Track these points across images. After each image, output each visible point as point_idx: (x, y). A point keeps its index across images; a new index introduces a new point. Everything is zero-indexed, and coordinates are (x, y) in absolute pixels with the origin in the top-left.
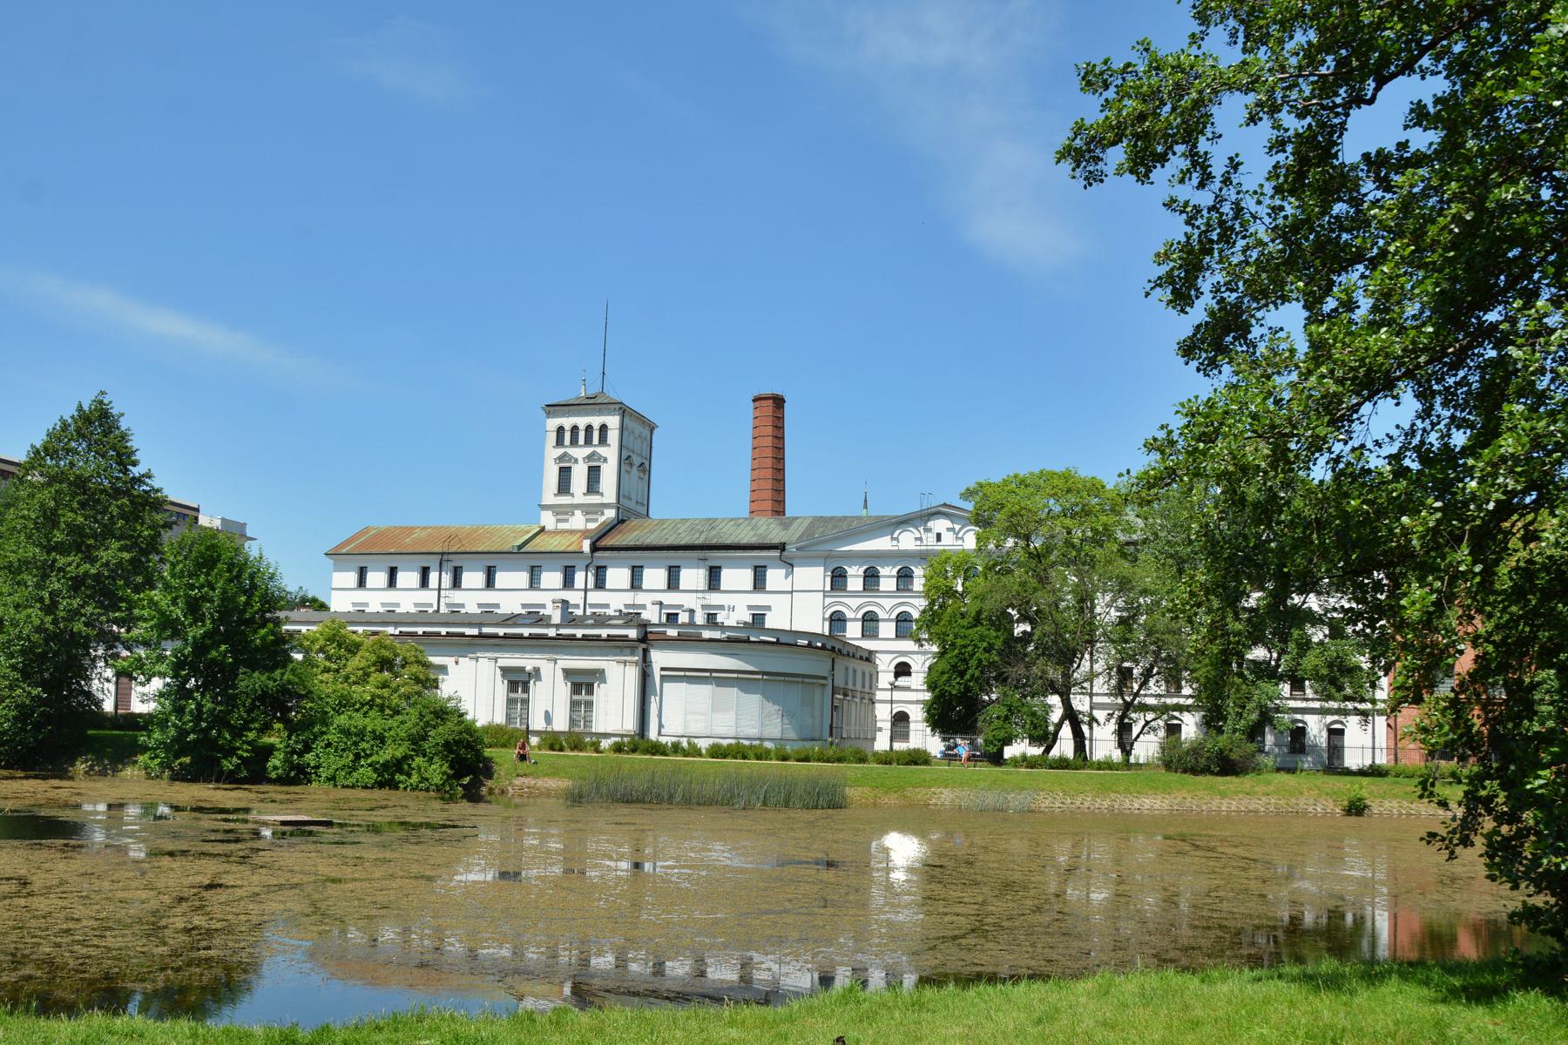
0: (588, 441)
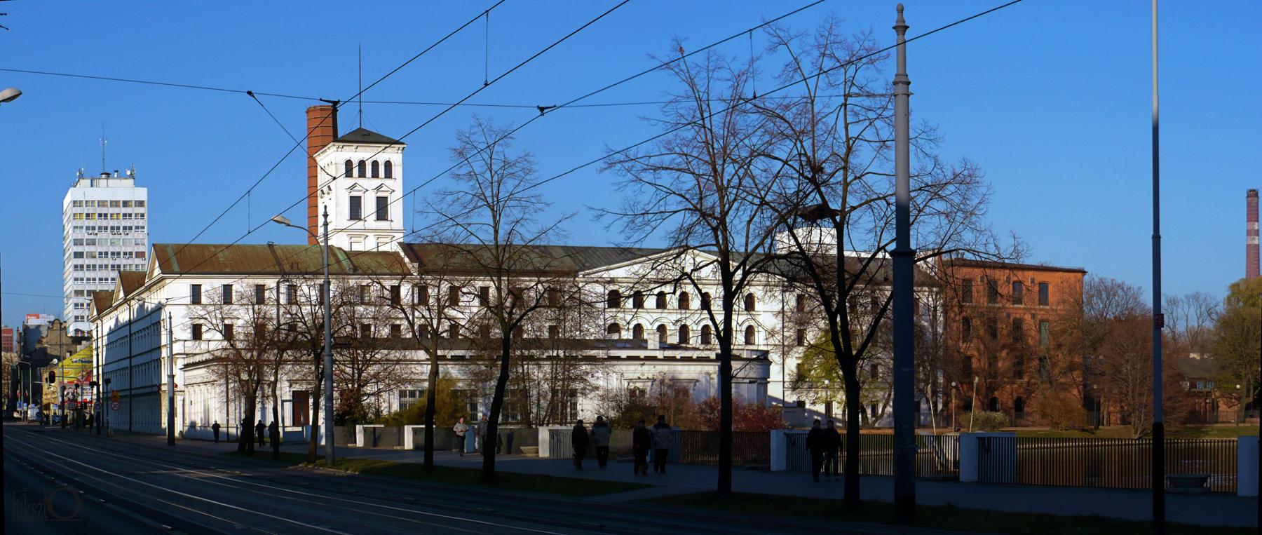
0: (375, 175)
